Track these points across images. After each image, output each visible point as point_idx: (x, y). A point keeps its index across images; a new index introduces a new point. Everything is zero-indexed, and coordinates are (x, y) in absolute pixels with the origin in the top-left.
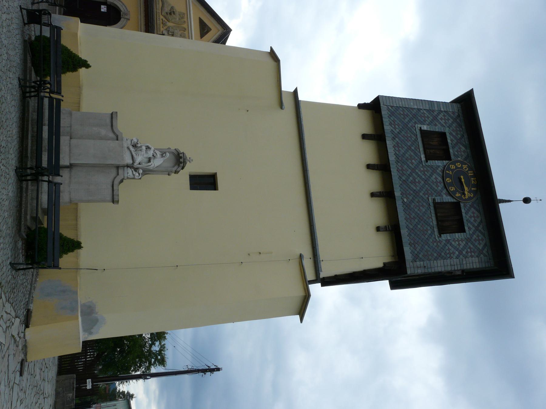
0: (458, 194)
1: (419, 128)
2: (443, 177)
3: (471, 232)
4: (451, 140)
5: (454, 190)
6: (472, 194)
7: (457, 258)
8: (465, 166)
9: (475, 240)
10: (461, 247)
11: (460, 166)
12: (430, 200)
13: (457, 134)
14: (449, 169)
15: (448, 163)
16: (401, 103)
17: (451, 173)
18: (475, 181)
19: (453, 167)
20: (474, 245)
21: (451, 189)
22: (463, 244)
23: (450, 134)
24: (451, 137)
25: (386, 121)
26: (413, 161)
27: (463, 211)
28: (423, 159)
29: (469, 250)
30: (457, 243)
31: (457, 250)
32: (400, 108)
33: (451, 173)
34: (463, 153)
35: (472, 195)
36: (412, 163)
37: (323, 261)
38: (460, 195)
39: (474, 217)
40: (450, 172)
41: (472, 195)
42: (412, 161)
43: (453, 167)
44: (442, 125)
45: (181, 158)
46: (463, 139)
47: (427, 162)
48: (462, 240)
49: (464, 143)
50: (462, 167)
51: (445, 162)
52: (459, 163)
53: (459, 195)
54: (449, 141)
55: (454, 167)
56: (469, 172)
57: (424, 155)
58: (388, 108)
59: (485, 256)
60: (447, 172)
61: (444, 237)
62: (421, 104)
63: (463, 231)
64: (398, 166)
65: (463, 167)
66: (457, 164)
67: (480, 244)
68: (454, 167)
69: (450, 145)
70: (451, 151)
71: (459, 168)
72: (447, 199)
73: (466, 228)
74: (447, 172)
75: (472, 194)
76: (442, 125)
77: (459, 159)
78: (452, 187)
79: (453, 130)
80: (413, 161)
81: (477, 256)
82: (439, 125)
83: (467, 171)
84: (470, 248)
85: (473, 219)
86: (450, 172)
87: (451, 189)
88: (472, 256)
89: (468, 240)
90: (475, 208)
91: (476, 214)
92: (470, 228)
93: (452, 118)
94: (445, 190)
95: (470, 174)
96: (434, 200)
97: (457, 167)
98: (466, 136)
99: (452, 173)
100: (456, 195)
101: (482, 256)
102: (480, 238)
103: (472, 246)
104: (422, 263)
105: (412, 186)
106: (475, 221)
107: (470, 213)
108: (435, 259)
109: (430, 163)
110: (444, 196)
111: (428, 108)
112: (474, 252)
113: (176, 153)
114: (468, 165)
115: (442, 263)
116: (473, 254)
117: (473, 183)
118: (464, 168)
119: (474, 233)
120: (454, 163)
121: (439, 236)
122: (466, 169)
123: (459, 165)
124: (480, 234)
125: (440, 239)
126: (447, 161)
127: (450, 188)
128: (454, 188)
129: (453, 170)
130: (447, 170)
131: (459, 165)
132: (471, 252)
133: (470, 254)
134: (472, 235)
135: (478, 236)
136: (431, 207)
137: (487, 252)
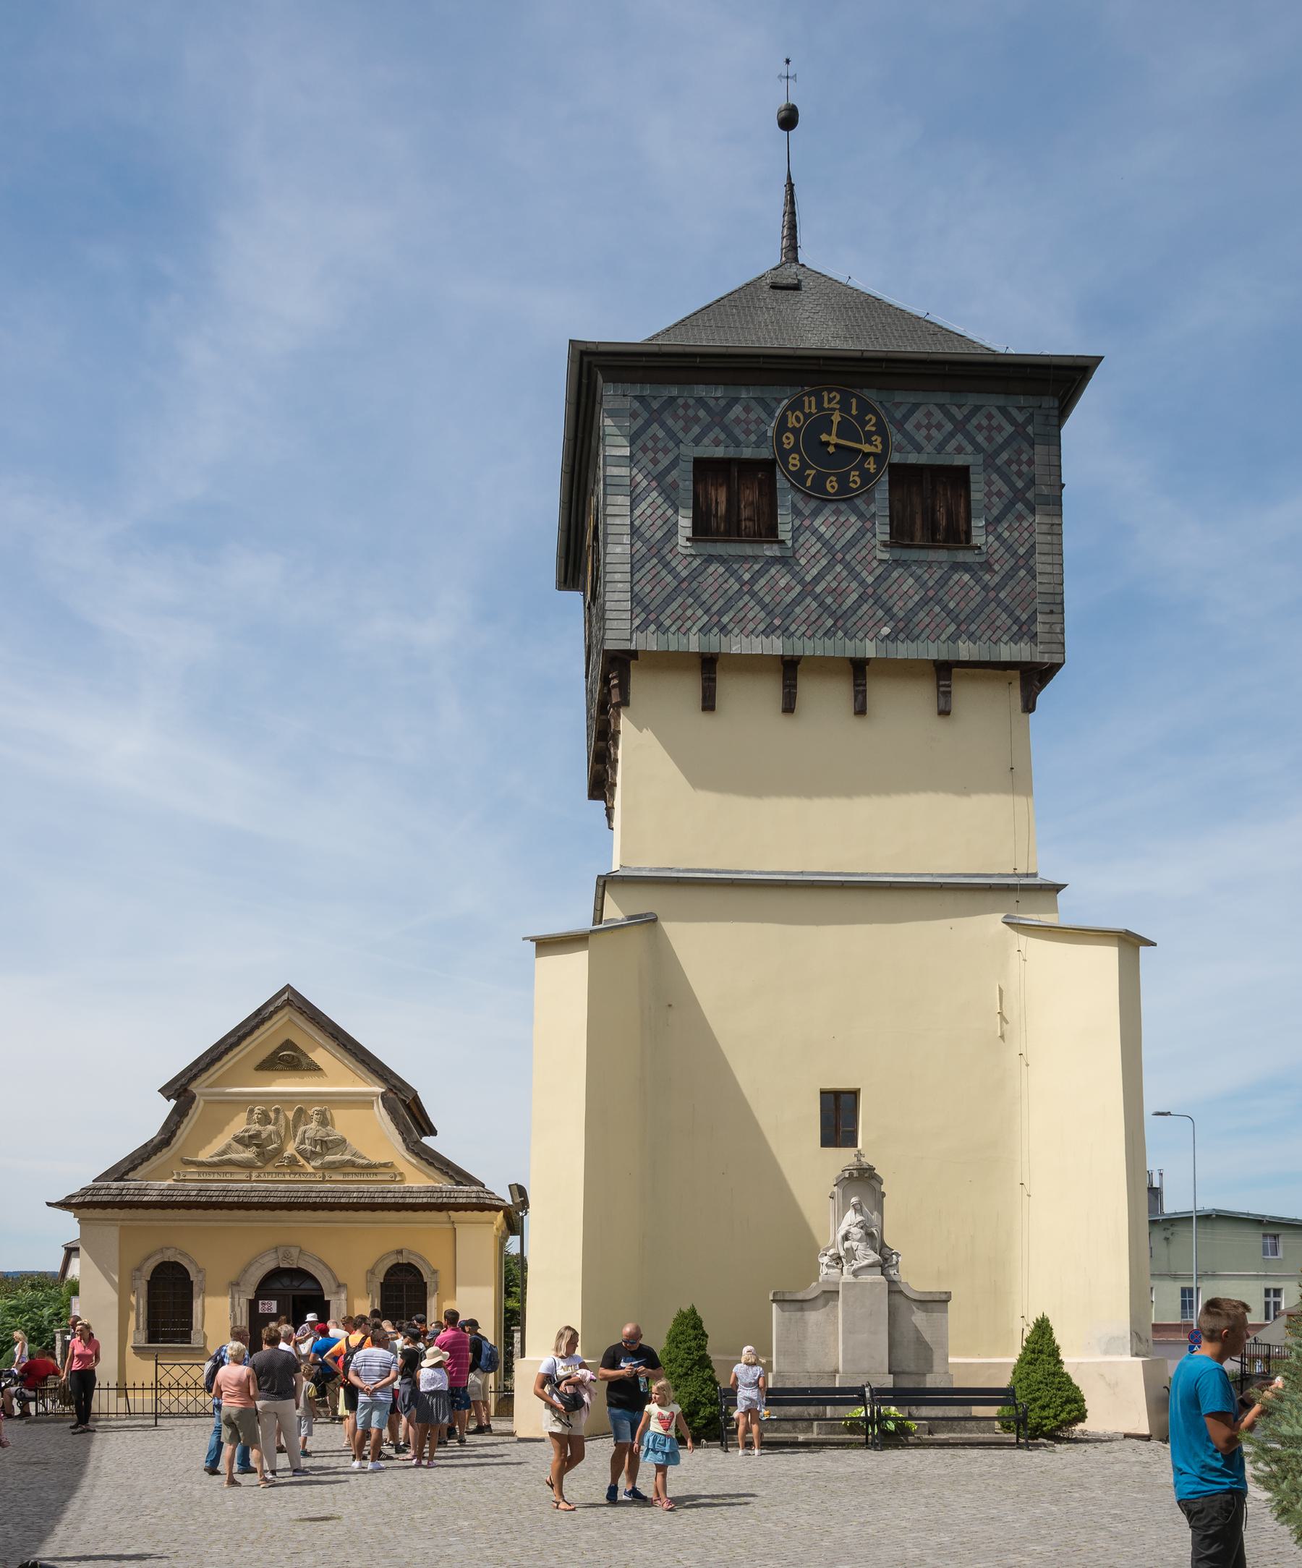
0: (869, 464)
1: (688, 544)
2: (823, 500)
3: (969, 448)
4: (717, 443)
5: (857, 473)
6: (867, 418)
8: (792, 422)
9: (990, 439)
10: (1005, 489)
11: (788, 434)
12: (886, 556)
13: (697, 420)
14: (799, 476)
15: (786, 476)
16: (620, 585)
17: (813, 472)
18: (831, 396)
19: (794, 460)
20: (1002, 448)
21: (855, 482)
22: (999, 484)
23: (697, 441)
24: (706, 441)
25: (675, 643)
27: (913, 458)
28: (771, 551)
29: (1014, 467)
30: (995, 499)
31: (1012, 504)
32: (636, 589)
33: (813, 472)
34: (753, 416)
35: (870, 420)
36: (788, 588)
39: (929, 427)
40: (809, 475)
41: (870, 420)
43: (794, 460)
44: (674, 464)
45: (851, 1174)
46: (712, 403)
48: (989, 483)
49: (722, 403)
50: (795, 431)
51: (781, 482)
52: (784, 439)
54: (719, 452)
55: (793, 455)
56: (807, 410)
57: (766, 546)
58: (637, 627)
59: (1030, 420)
60: (809, 484)
61: (978, 538)
62: (618, 521)
63: (965, 470)
64: (798, 633)
66: (788, 447)
67: (1000, 429)
68: (795, 459)
69: (732, 453)
70: (747, 453)
71: (797, 441)
73: (959, 461)
74: (809, 484)
75: (867, 418)
76: (674, 464)
77: (770, 434)
79: (686, 430)
81: (1032, 445)
82: (674, 473)
83: (807, 416)
84: (1009, 463)
85: (934, 432)
86: (809, 475)
87: (855, 482)
88: (1031, 462)
89: (989, 463)
90: (906, 417)
91: (919, 415)
92: (959, 450)
93: (647, 424)
94: (858, 502)
95: (814, 410)
96: (884, 544)
97: (795, 449)
98: (700, 391)
99: (814, 469)
100: (872, 471)
101: (1030, 429)
102: (985, 423)
103: (1005, 456)
104: (1040, 618)
105: (849, 602)
106: (939, 427)
107: (920, 436)
108: (1034, 578)
109: (784, 531)
110: (873, 508)
111: (627, 501)
112: (1019, 452)
113: (846, 1182)
114: (786, 410)
115: (1044, 558)
116: (1024, 457)
117: (838, 406)
118: (798, 426)
119: (973, 441)
120: (785, 454)
121: (976, 552)
122: (798, 419)
123: (788, 438)
124: (974, 421)
125: (984, 549)
126: (779, 476)
127: (852, 485)
128: (853, 473)
129: (805, 466)
130: (804, 484)
131: (788, 438)
132: (1019, 463)
133: (1025, 468)
134: (978, 448)
135: (979, 427)
136: (903, 558)
137: (1020, 409)
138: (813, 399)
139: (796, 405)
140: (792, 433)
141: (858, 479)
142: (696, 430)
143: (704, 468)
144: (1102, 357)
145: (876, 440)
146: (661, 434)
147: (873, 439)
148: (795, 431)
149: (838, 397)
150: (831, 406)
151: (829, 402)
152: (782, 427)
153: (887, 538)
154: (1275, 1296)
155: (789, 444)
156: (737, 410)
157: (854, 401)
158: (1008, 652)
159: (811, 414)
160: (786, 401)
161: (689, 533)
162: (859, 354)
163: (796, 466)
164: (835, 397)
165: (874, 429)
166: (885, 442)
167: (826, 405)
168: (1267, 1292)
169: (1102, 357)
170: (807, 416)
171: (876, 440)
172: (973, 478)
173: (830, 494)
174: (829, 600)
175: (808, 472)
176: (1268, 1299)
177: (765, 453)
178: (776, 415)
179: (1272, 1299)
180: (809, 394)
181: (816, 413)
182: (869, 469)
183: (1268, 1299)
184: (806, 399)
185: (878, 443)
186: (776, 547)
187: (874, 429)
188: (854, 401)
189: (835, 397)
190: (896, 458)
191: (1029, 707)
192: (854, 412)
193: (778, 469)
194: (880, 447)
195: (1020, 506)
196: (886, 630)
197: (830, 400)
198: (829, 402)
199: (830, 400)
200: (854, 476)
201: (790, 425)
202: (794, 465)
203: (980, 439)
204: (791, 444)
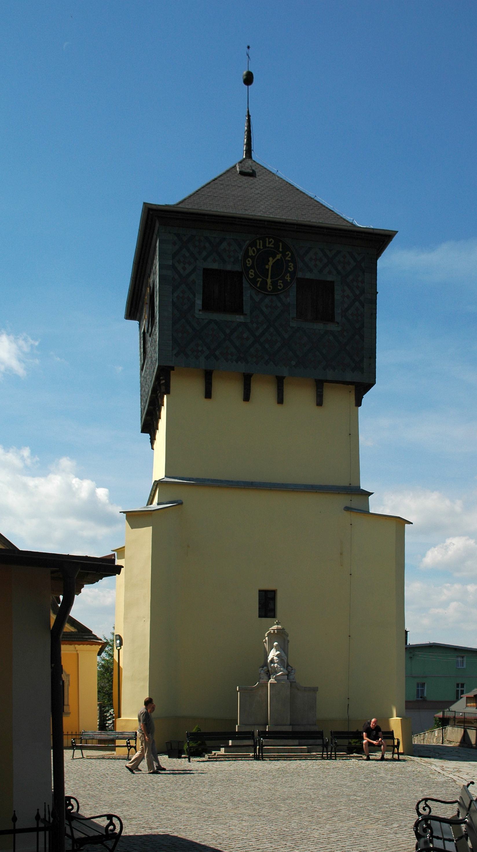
0: (287, 277)
1: (201, 313)
5: (281, 281)
6: (287, 253)
7: (363, 306)
8: (251, 253)
11: (249, 259)
17: (260, 280)
19: (252, 273)
21: (280, 286)
23: (205, 259)
26: (245, 336)
27: (308, 276)
33: (260, 280)
35: (288, 254)
37: (350, 484)
38: (288, 274)
40: (258, 281)
41: (289, 254)
42: (245, 337)
47: (246, 314)
50: (252, 258)
53: (289, 276)
55: (251, 270)
56: (258, 247)
60: (258, 285)
61: (338, 318)
63: (332, 283)
65: (252, 255)
70: (229, 268)
72: (291, 297)
73: (330, 278)
74: (258, 285)
75: (287, 253)
77: (240, 258)
78: (279, 284)
80: (245, 336)
87: (280, 286)
95: (261, 248)
96: (293, 318)
97: (252, 267)
100: (289, 281)
109: (247, 308)
117: (273, 246)
118: (253, 255)
121: (336, 325)
122: (254, 252)
123: (249, 261)
126: (244, 280)
127: (279, 287)
128: (280, 281)
131: (249, 261)
138: (261, 241)
139: (253, 244)
140: (251, 259)
141: (281, 284)
142: (204, 254)
143: (207, 272)
144: (397, 232)
145: (291, 265)
146: (187, 254)
147: (290, 264)
148: (252, 258)
149: (273, 241)
150: (270, 246)
151: (269, 244)
152: (246, 255)
153: (295, 315)
154: (461, 687)
155: (249, 264)
156: (224, 245)
157: (281, 244)
158: (349, 376)
159: (260, 249)
160: (248, 242)
161: (200, 307)
162: (284, 220)
163: (252, 276)
164: (272, 241)
165: (290, 259)
166: (295, 267)
167: (267, 245)
168: (458, 685)
169: (397, 232)
170: (258, 250)
171: (291, 265)
172: (336, 288)
173: (269, 292)
174: (267, 346)
175: (258, 279)
176: (458, 689)
177: (237, 268)
178: (243, 248)
179: (460, 689)
180: (259, 239)
181: (262, 249)
182: (287, 280)
183: (458, 689)
184: (258, 241)
185: (291, 267)
186: (242, 317)
187: (290, 259)
188: (281, 244)
189: (272, 241)
190: (300, 275)
191: (359, 403)
192: (281, 250)
193: (244, 277)
194: (293, 269)
195: (357, 304)
196: (293, 363)
197: (269, 243)
198: (269, 244)
199: (269, 243)
200: (280, 283)
201: (250, 254)
202: (252, 275)
203: (340, 268)
204: (251, 264)
